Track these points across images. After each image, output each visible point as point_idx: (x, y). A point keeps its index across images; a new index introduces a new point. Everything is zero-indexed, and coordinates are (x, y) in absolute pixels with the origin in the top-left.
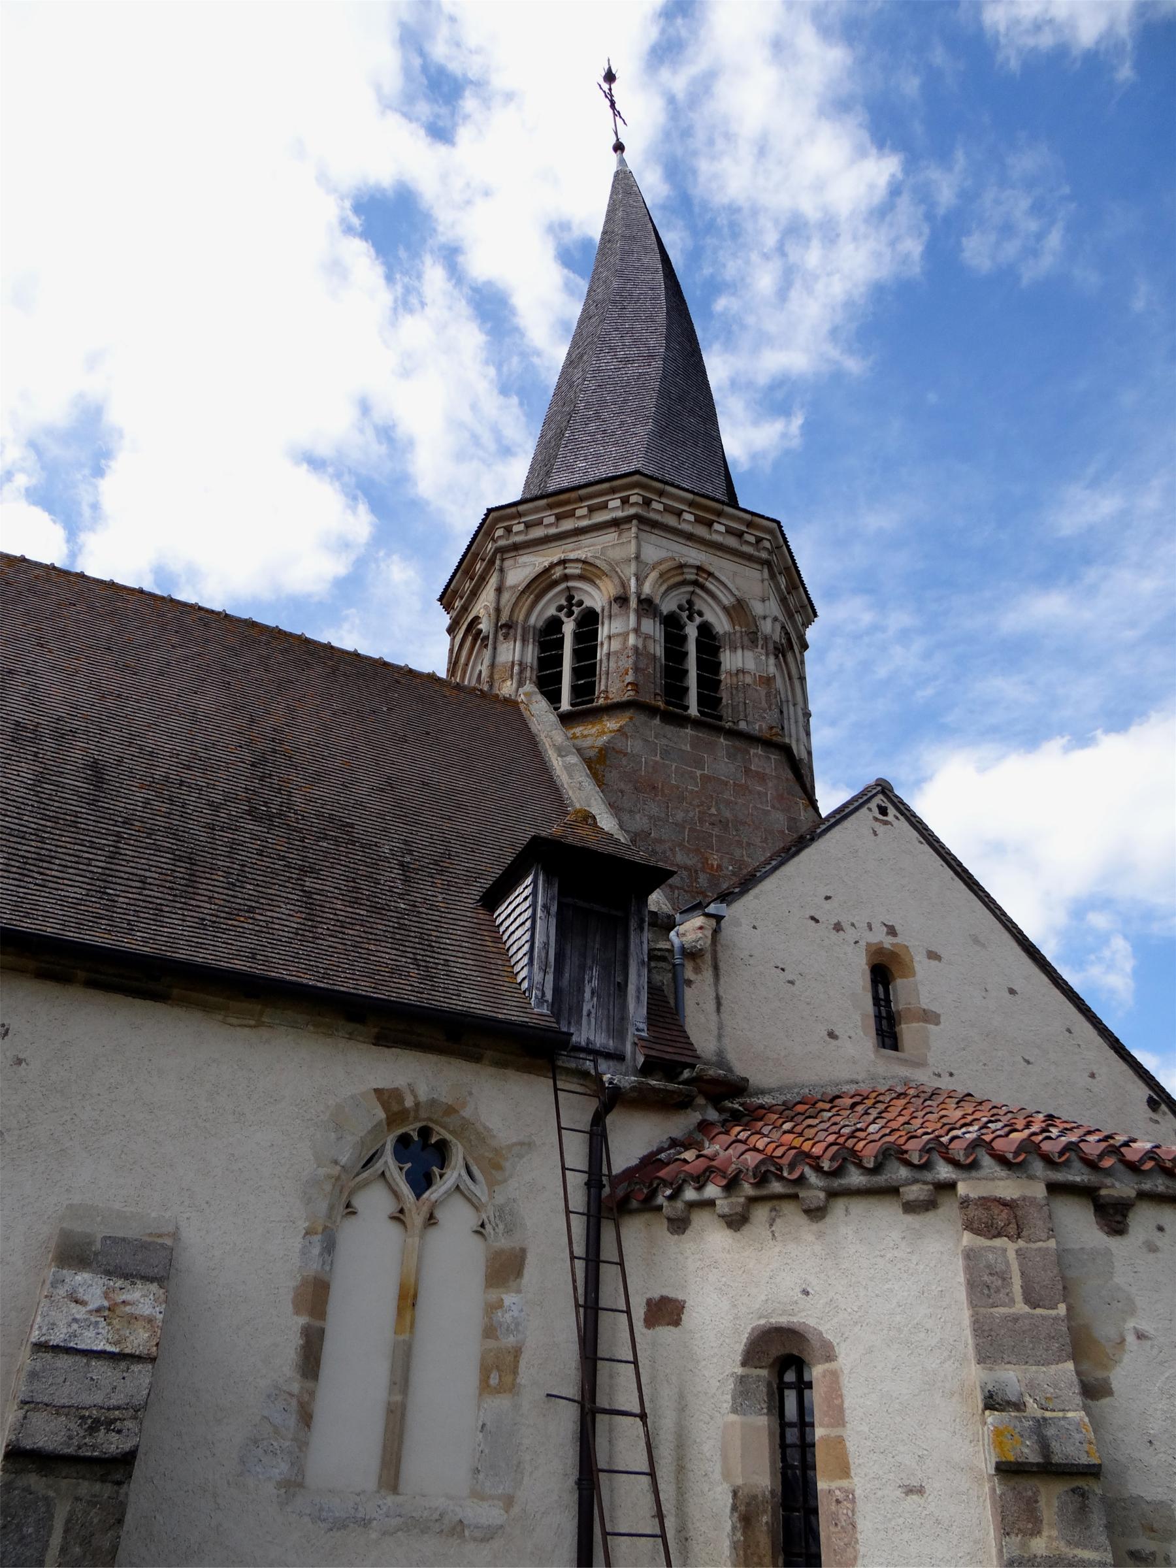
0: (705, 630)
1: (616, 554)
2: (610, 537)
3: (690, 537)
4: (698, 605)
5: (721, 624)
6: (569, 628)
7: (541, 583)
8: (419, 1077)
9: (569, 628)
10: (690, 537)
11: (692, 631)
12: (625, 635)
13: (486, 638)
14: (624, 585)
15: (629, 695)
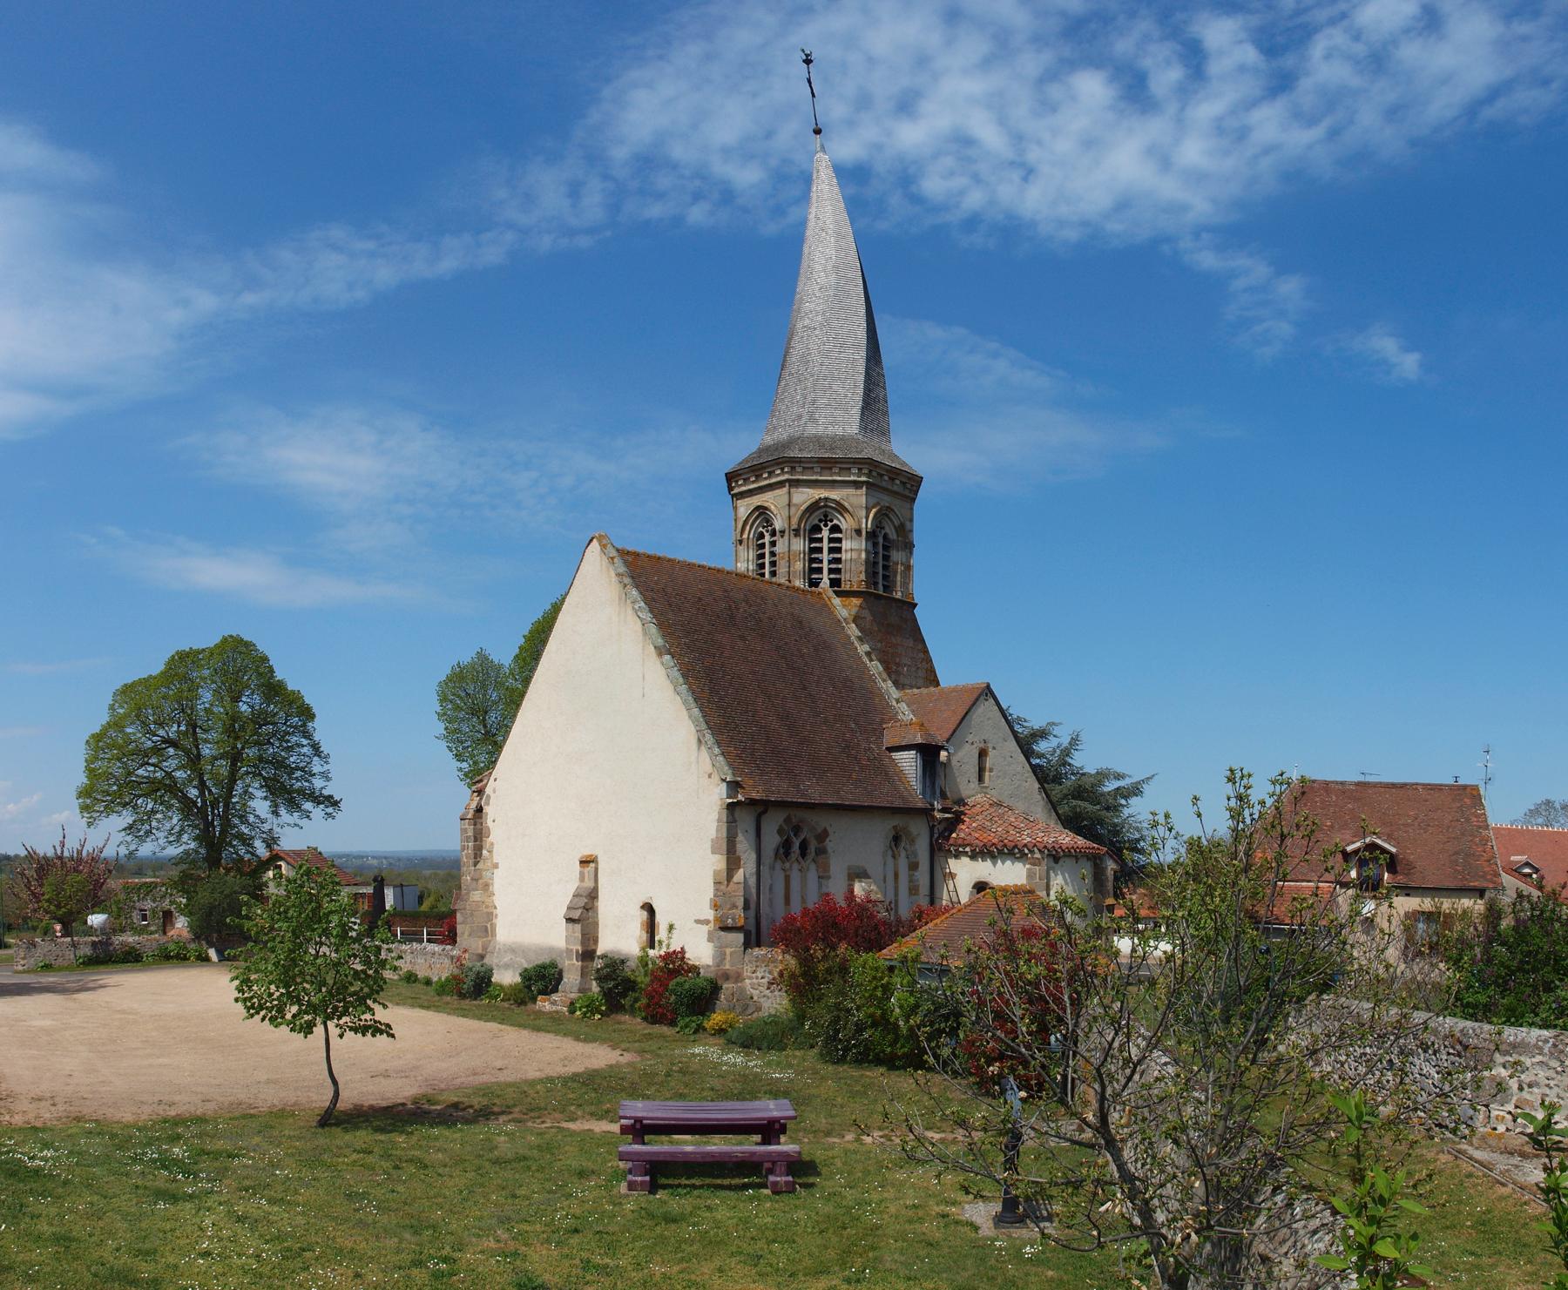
0: (885, 537)
1: (854, 500)
2: (851, 491)
3: (885, 490)
4: (884, 524)
5: (893, 535)
6: (825, 533)
7: (814, 507)
8: (897, 821)
9: (825, 533)
10: (885, 490)
11: (881, 540)
12: (859, 551)
13: (782, 532)
14: (859, 522)
15: (863, 588)
